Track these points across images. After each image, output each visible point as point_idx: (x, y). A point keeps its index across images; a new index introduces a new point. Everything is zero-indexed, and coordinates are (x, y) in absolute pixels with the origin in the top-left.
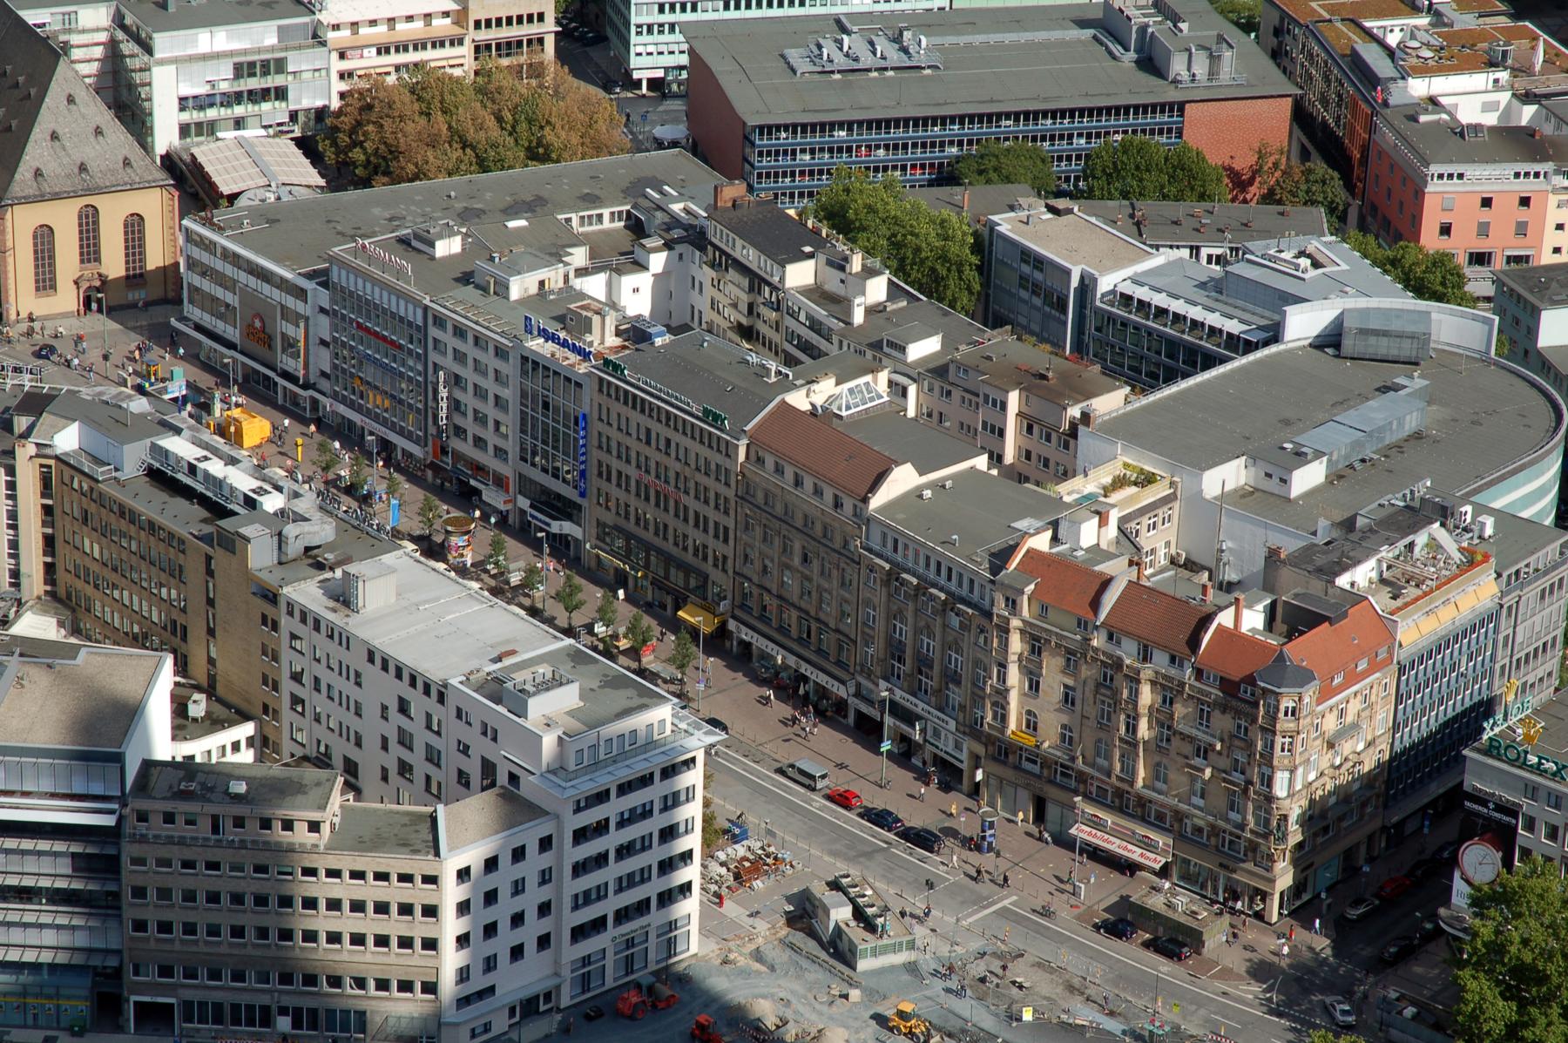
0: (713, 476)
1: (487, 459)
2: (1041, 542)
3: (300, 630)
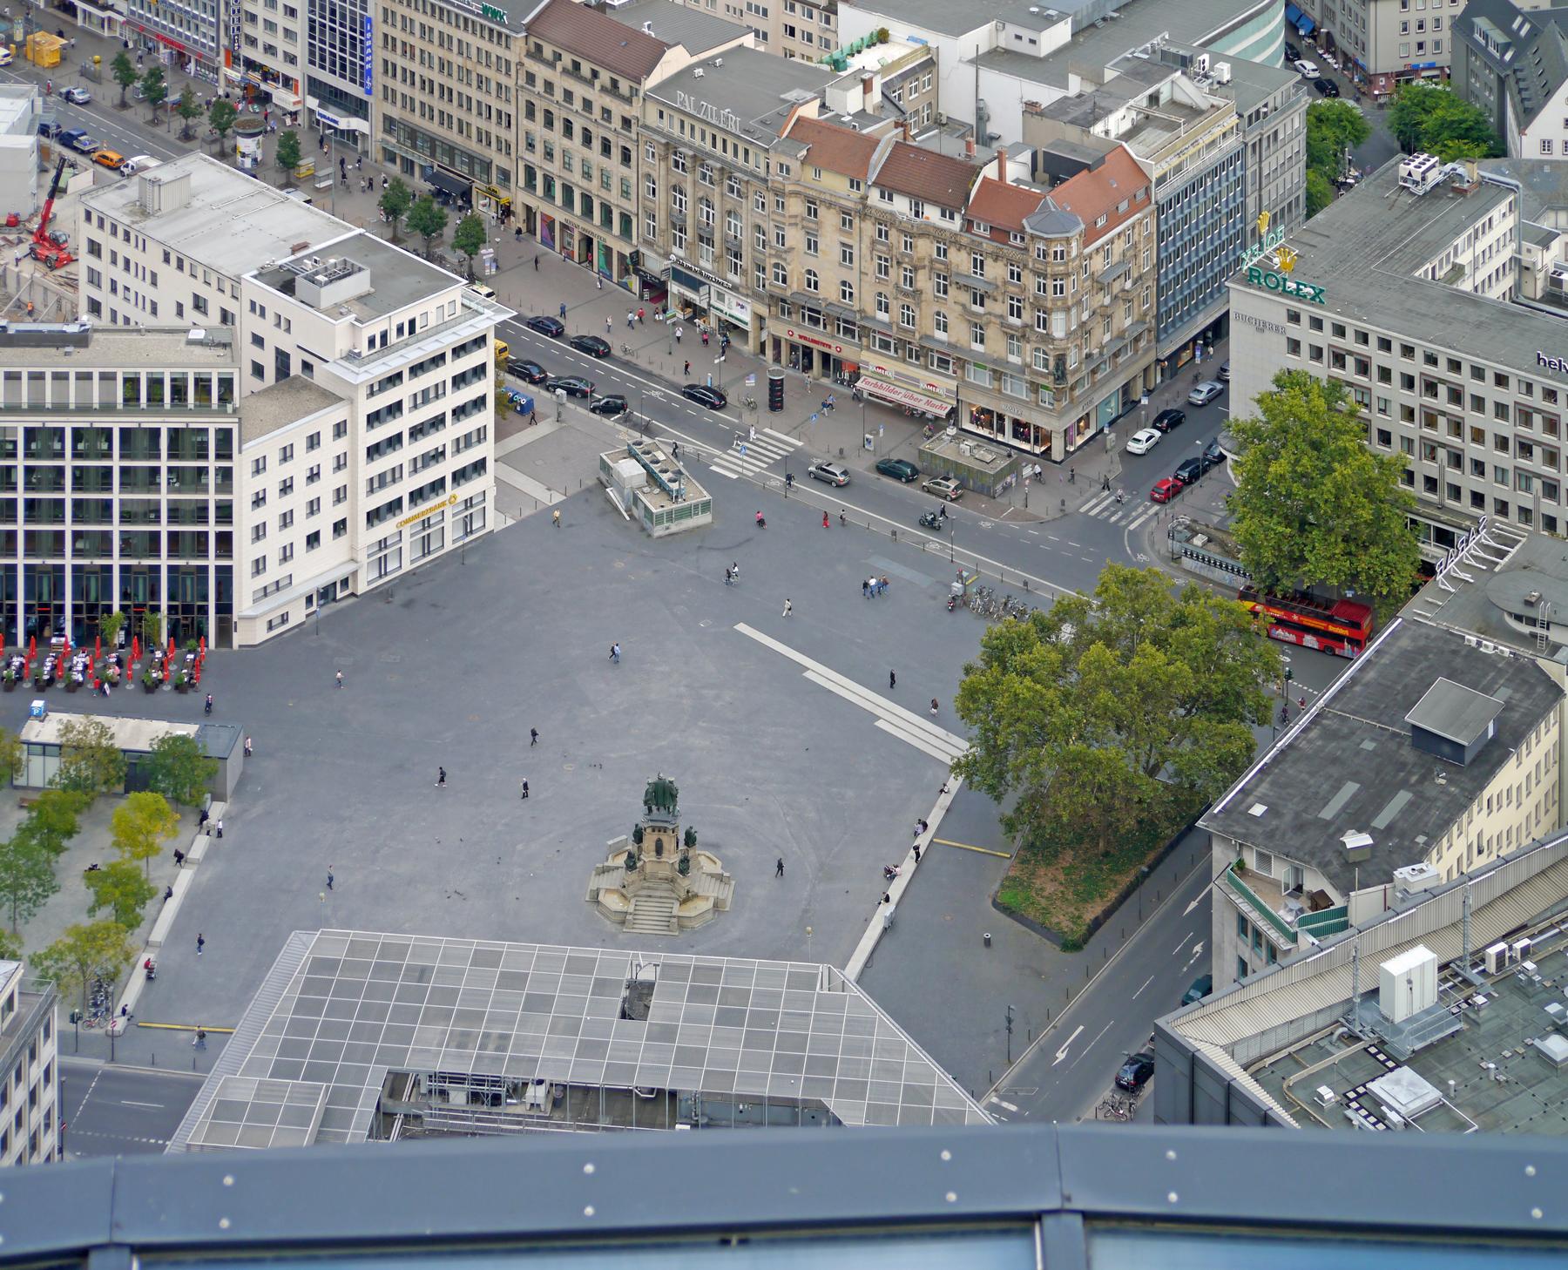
0: (494, 67)
1: (276, 64)
2: (810, 111)
3: (102, 237)
